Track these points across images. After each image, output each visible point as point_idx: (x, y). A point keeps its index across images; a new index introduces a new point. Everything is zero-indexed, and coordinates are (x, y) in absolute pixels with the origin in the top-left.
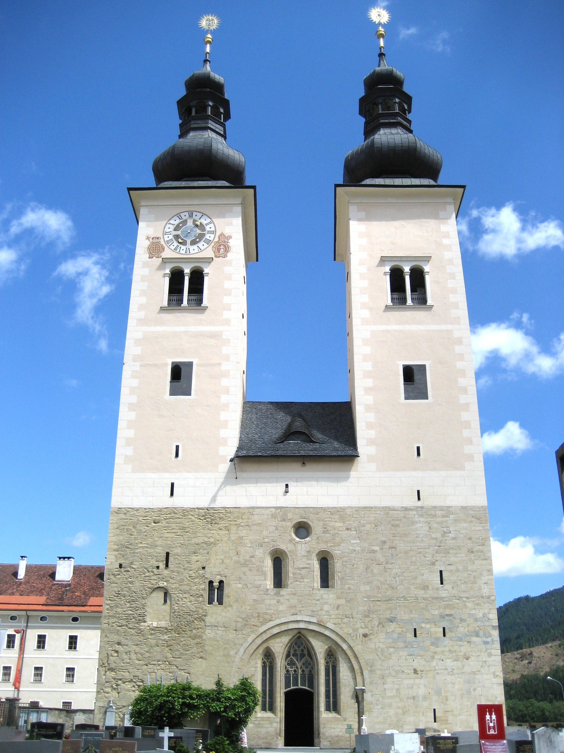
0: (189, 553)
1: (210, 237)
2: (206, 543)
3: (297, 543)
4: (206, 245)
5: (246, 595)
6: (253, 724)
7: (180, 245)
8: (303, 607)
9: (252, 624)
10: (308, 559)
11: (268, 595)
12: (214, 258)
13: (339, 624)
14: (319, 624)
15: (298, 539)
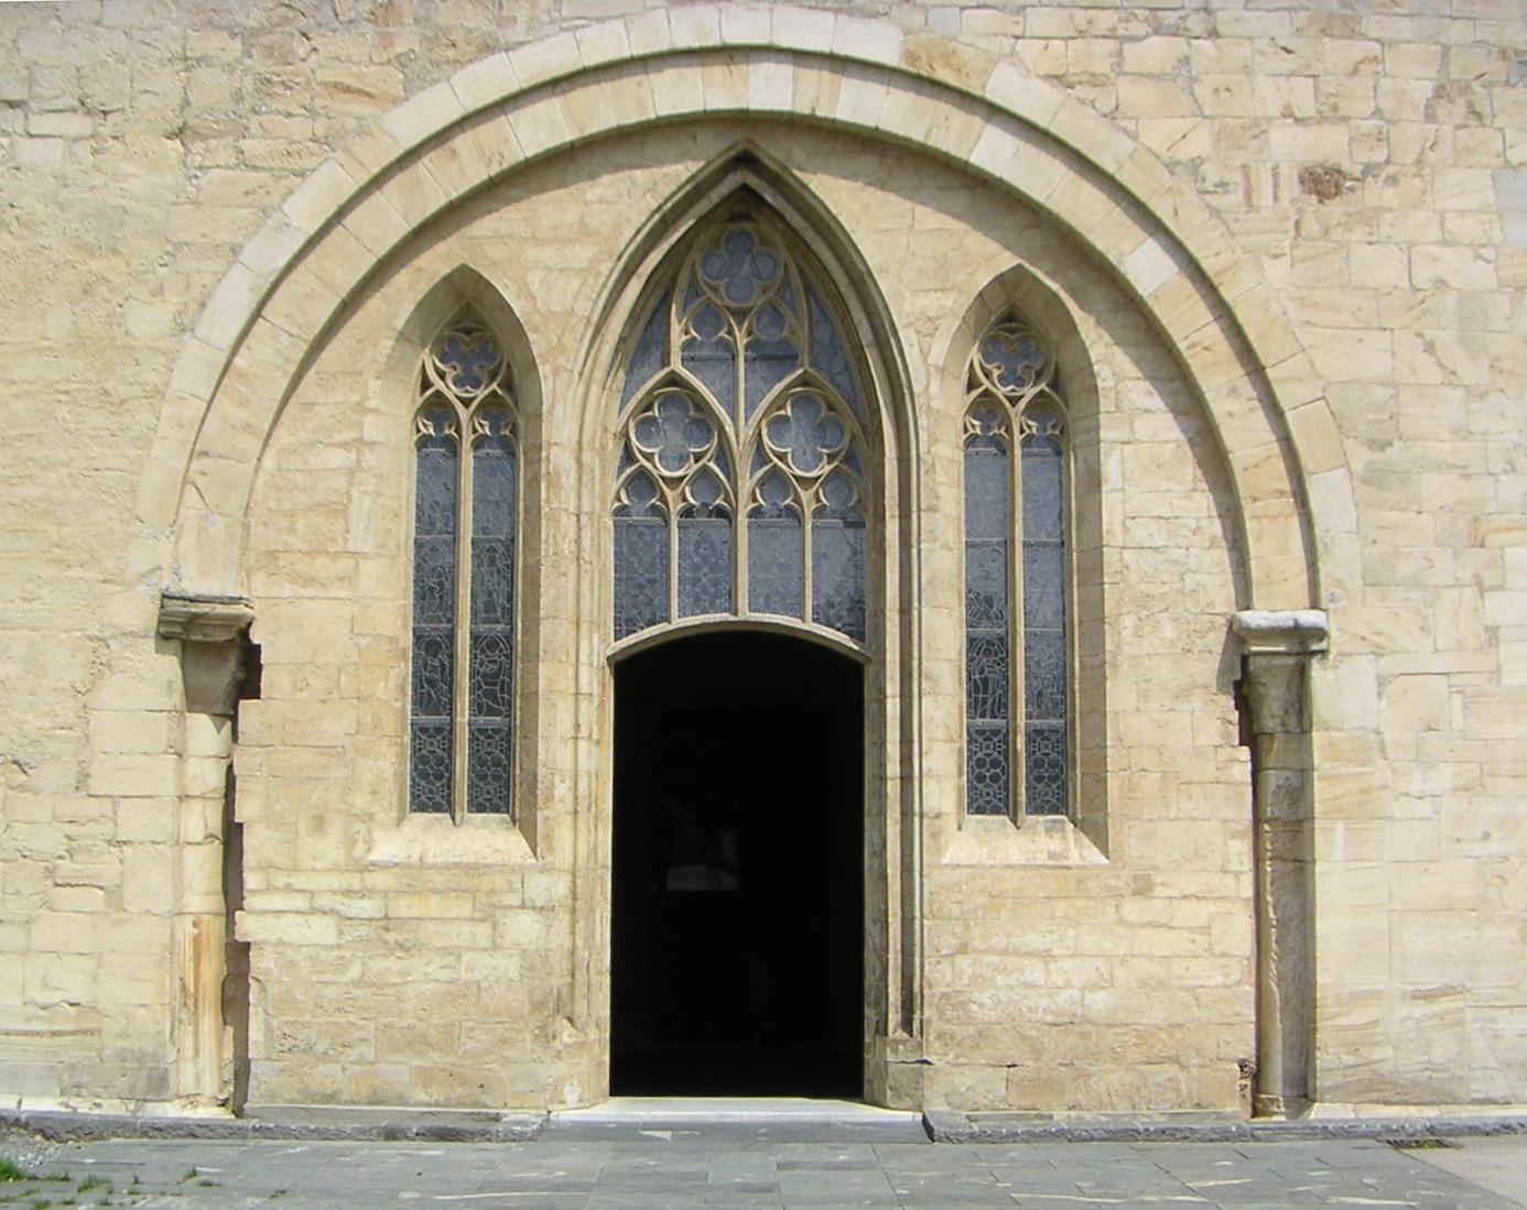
6: (327, 920)
9: (322, 75)
13: (1097, 81)
14: (918, 78)
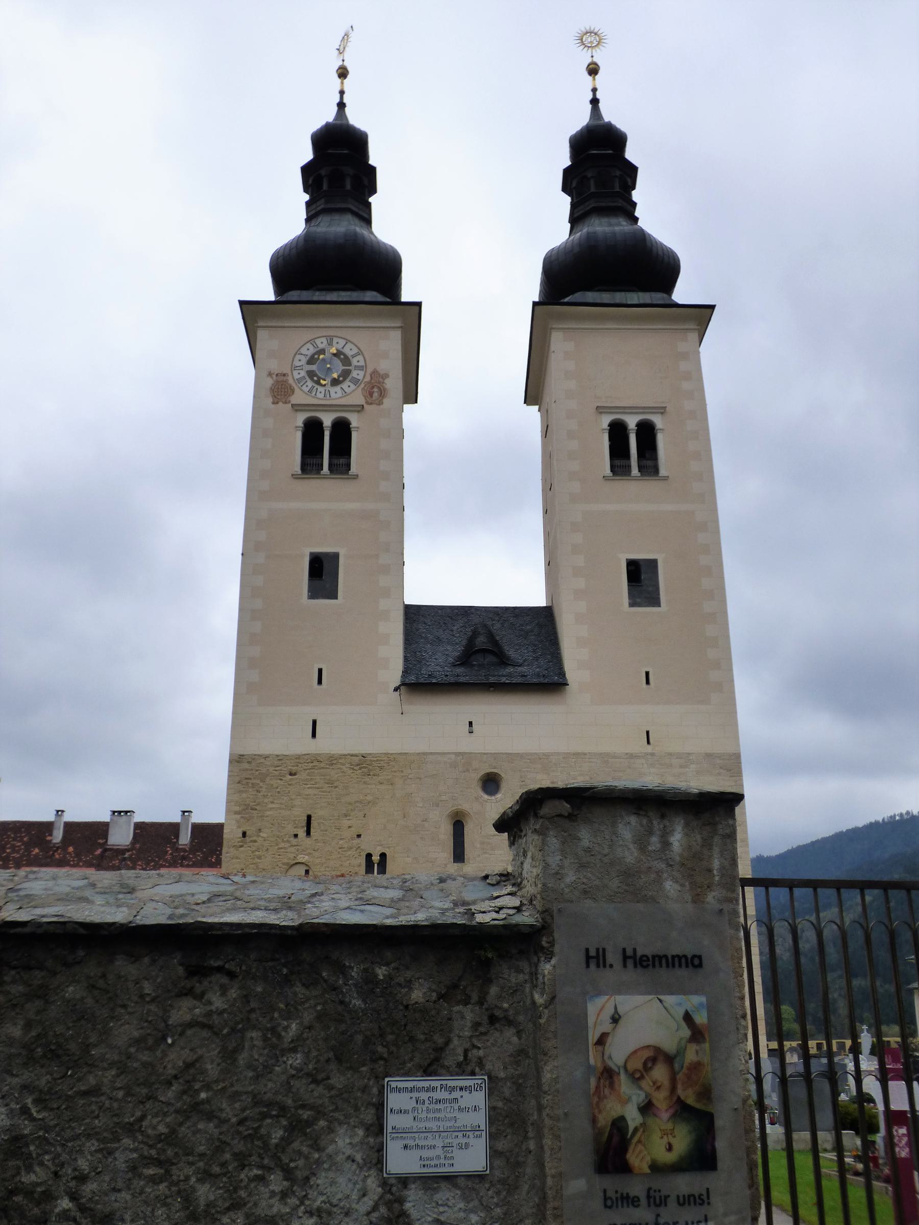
0: (339, 816)
1: (358, 374)
2: (360, 802)
3: (486, 801)
4: (353, 387)
7: (314, 385)
12: (365, 406)
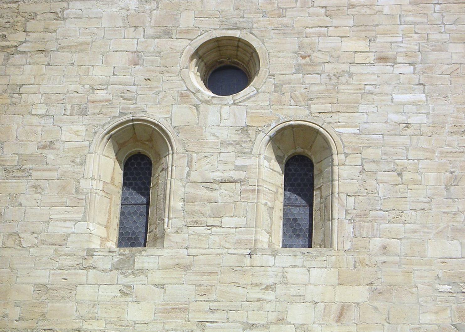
3: (207, 102)
5: (12, 269)
8: (212, 311)
10: (241, 153)
11: (91, 271)
15: (209, 94)
